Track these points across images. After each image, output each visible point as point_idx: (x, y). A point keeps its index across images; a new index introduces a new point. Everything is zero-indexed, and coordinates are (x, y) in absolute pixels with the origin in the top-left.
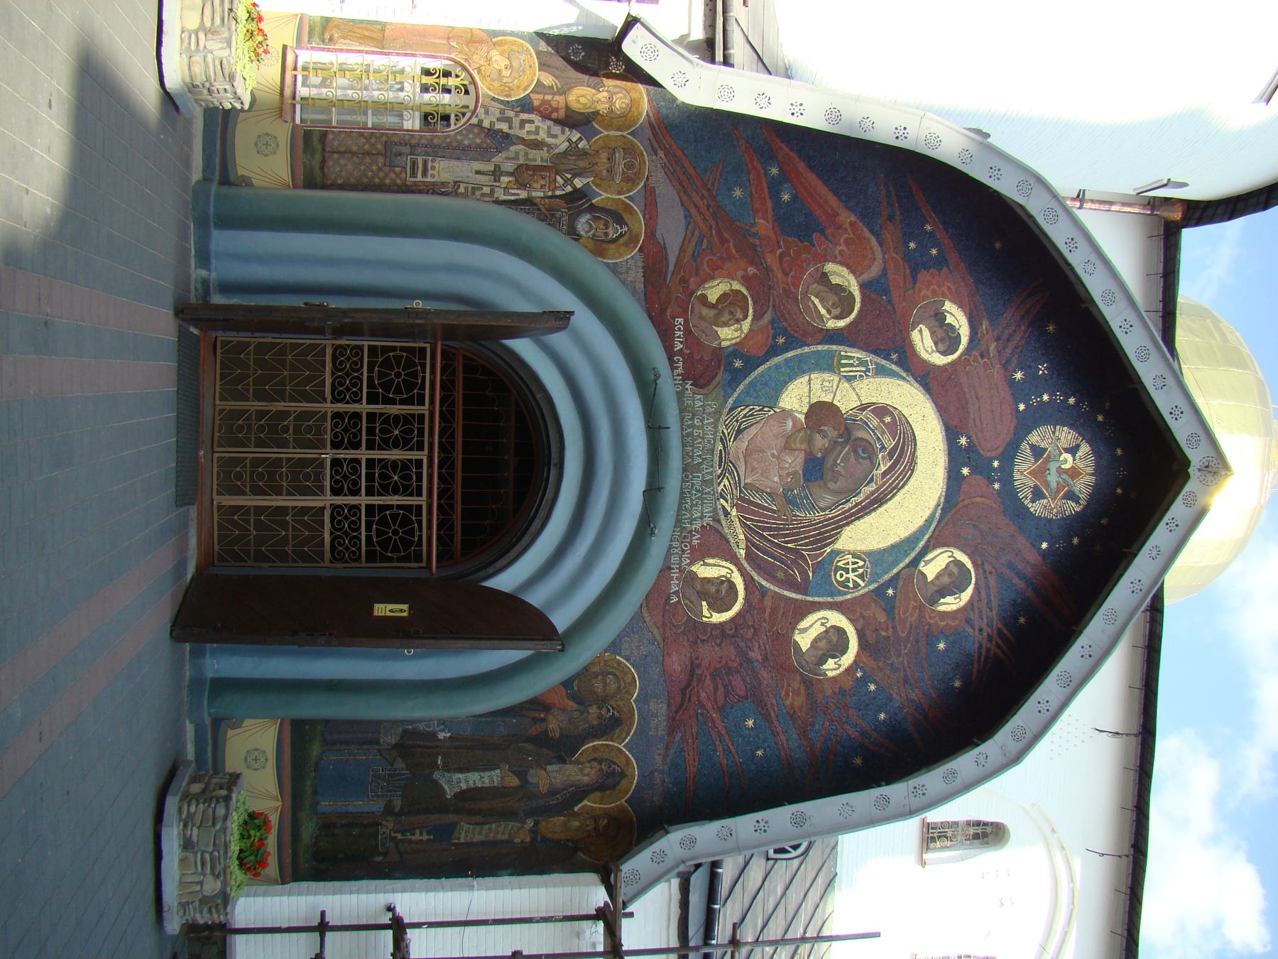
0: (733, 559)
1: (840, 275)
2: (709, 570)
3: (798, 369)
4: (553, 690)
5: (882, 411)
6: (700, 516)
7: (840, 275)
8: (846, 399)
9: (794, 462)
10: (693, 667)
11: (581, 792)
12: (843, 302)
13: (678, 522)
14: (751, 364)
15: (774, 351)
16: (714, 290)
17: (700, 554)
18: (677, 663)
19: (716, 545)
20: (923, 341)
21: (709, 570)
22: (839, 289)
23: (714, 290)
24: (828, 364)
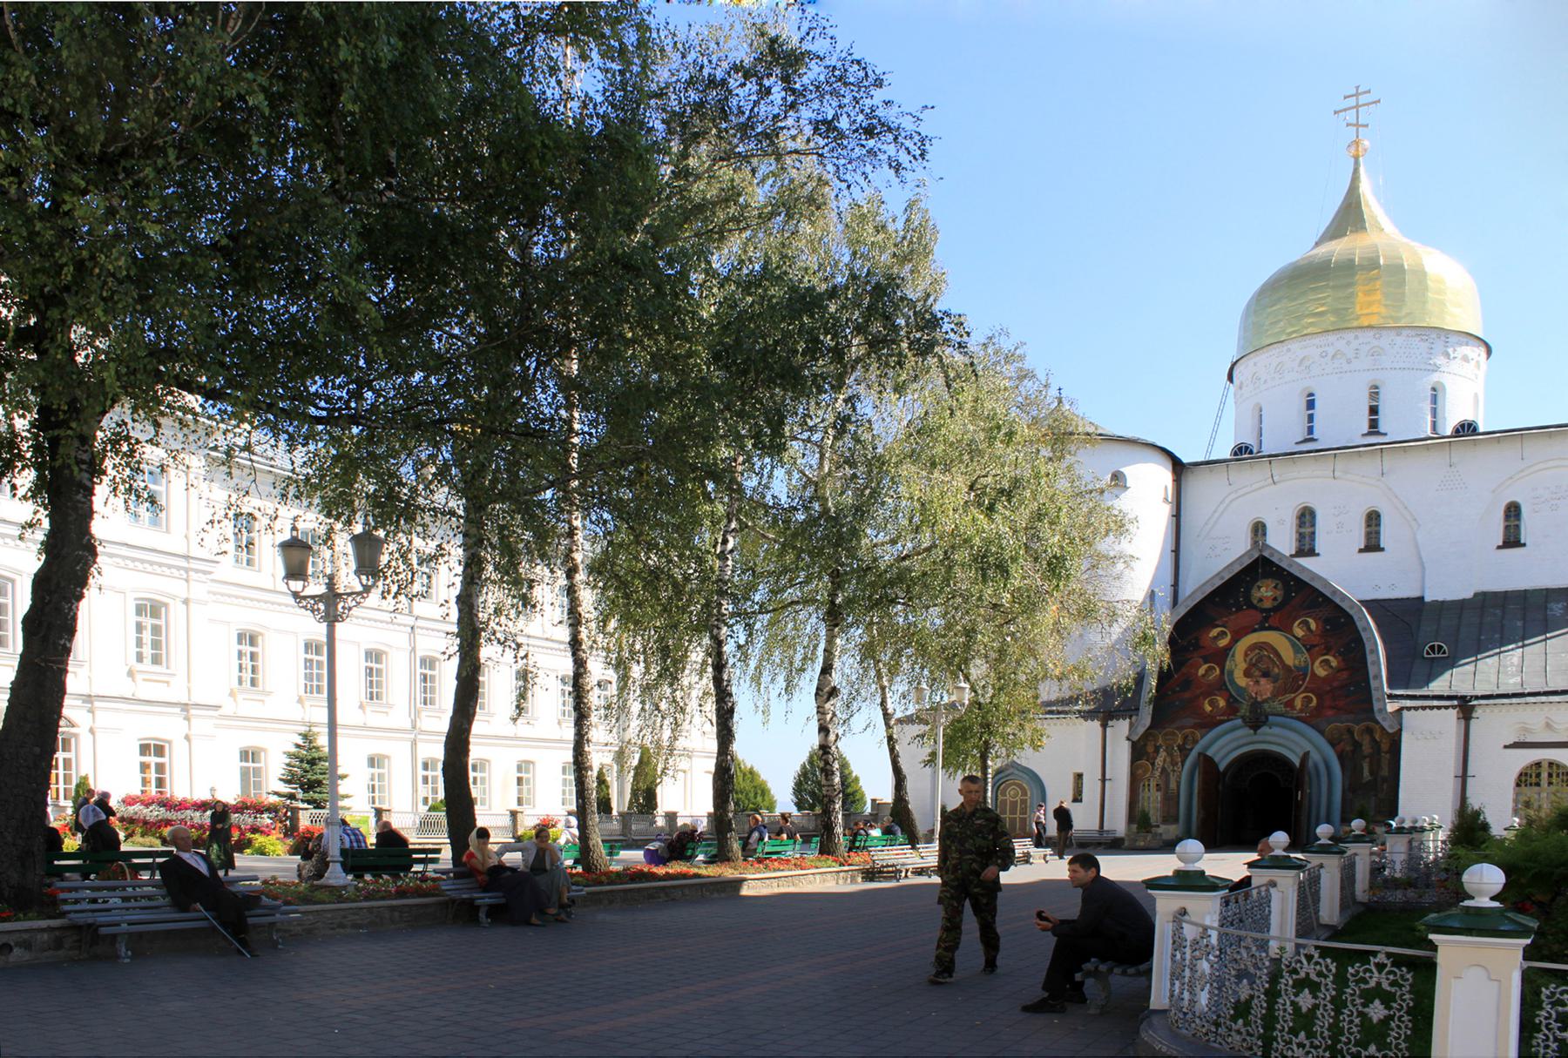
0: (1293, 699)
1: (1201, 671)
2: (1298, 703)
3: (1233, 682)
4: (1336, 751)
5: (1246, 655)
6: (1281, 708)
7: (1201, 671)
8: (1243, 666)
9: (1263, 681)
10: (1331, 707)
11: (1373, 740)
12: (1210, 669)
13: (1282, 715)
14: (1231, 696)
15: (1227, 690)
16: (1208, 708)
17: (1293, 708)
18: (1330, 713)
19: (1290, 704)
20: (1223, 643)
21: (1298, 703)
22: (1206, 671)
23: (1208, 708)
24: (1231, 673)
